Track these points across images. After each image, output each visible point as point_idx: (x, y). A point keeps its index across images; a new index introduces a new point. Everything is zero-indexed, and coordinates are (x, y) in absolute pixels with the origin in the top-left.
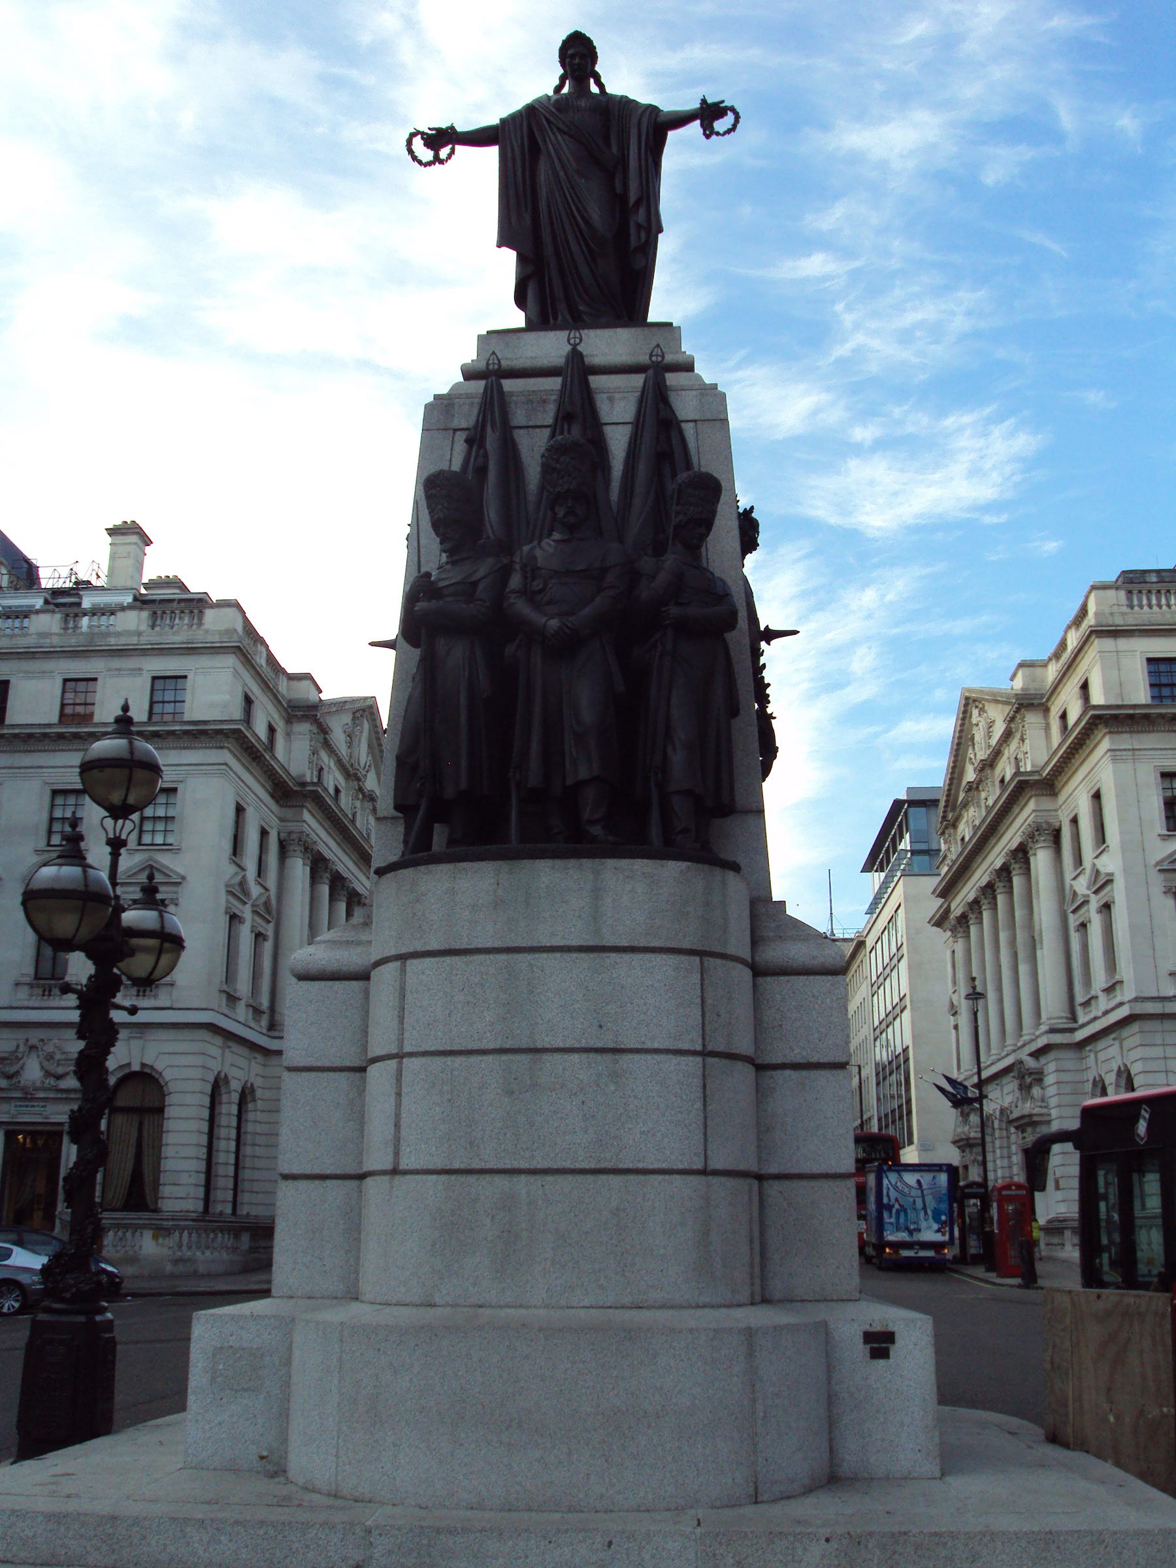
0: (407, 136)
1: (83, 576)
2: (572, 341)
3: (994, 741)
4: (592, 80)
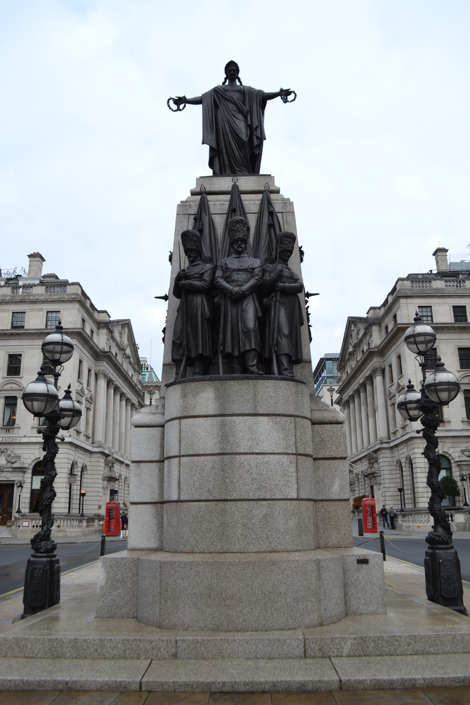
0: (167, 100)
1: (18, 272)
2: (234, 181)
3: (360, 336)
4: (237, 80)
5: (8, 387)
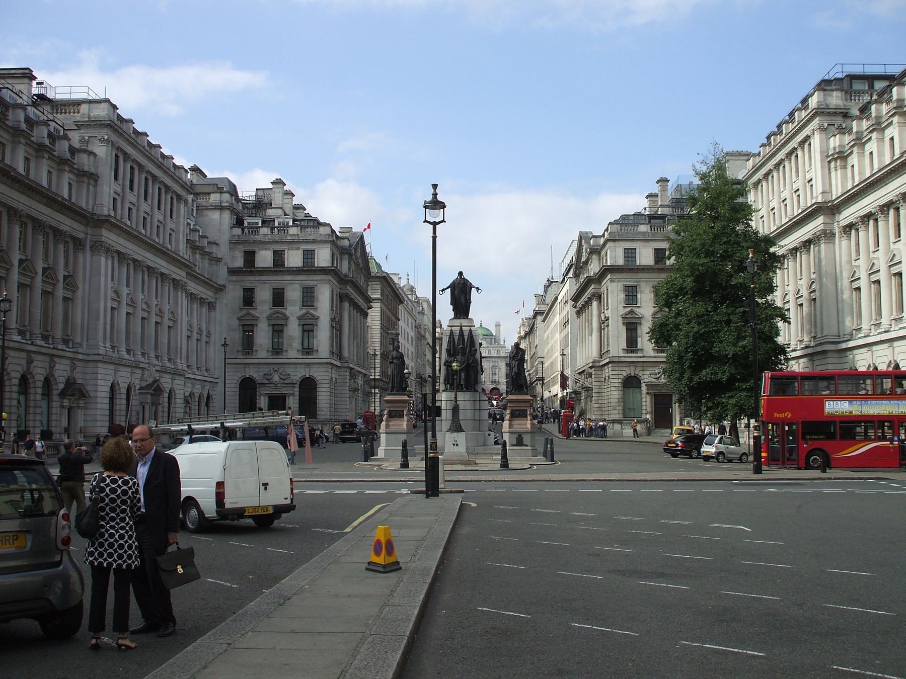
5: (276, 316)
